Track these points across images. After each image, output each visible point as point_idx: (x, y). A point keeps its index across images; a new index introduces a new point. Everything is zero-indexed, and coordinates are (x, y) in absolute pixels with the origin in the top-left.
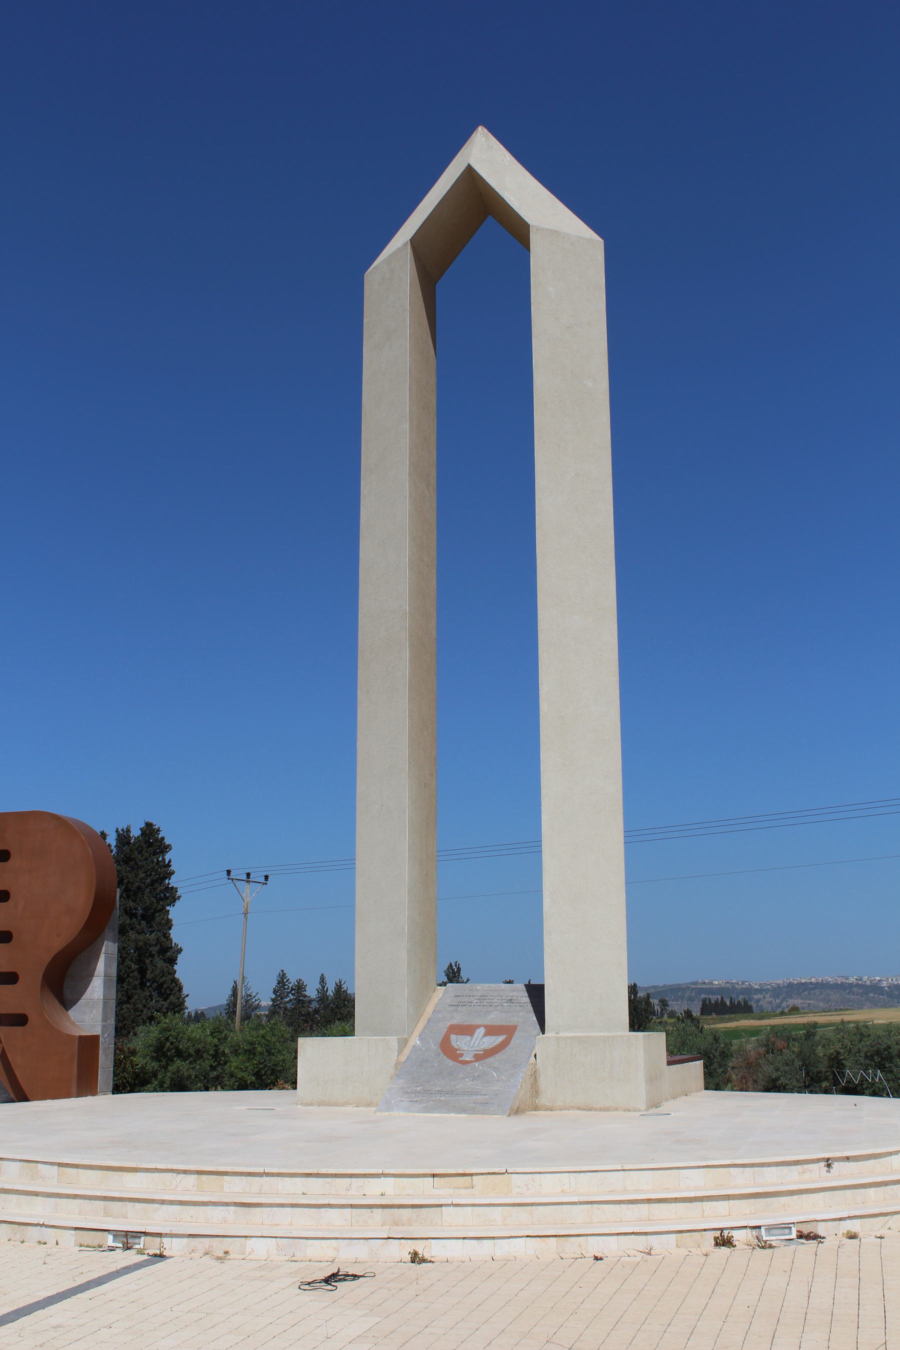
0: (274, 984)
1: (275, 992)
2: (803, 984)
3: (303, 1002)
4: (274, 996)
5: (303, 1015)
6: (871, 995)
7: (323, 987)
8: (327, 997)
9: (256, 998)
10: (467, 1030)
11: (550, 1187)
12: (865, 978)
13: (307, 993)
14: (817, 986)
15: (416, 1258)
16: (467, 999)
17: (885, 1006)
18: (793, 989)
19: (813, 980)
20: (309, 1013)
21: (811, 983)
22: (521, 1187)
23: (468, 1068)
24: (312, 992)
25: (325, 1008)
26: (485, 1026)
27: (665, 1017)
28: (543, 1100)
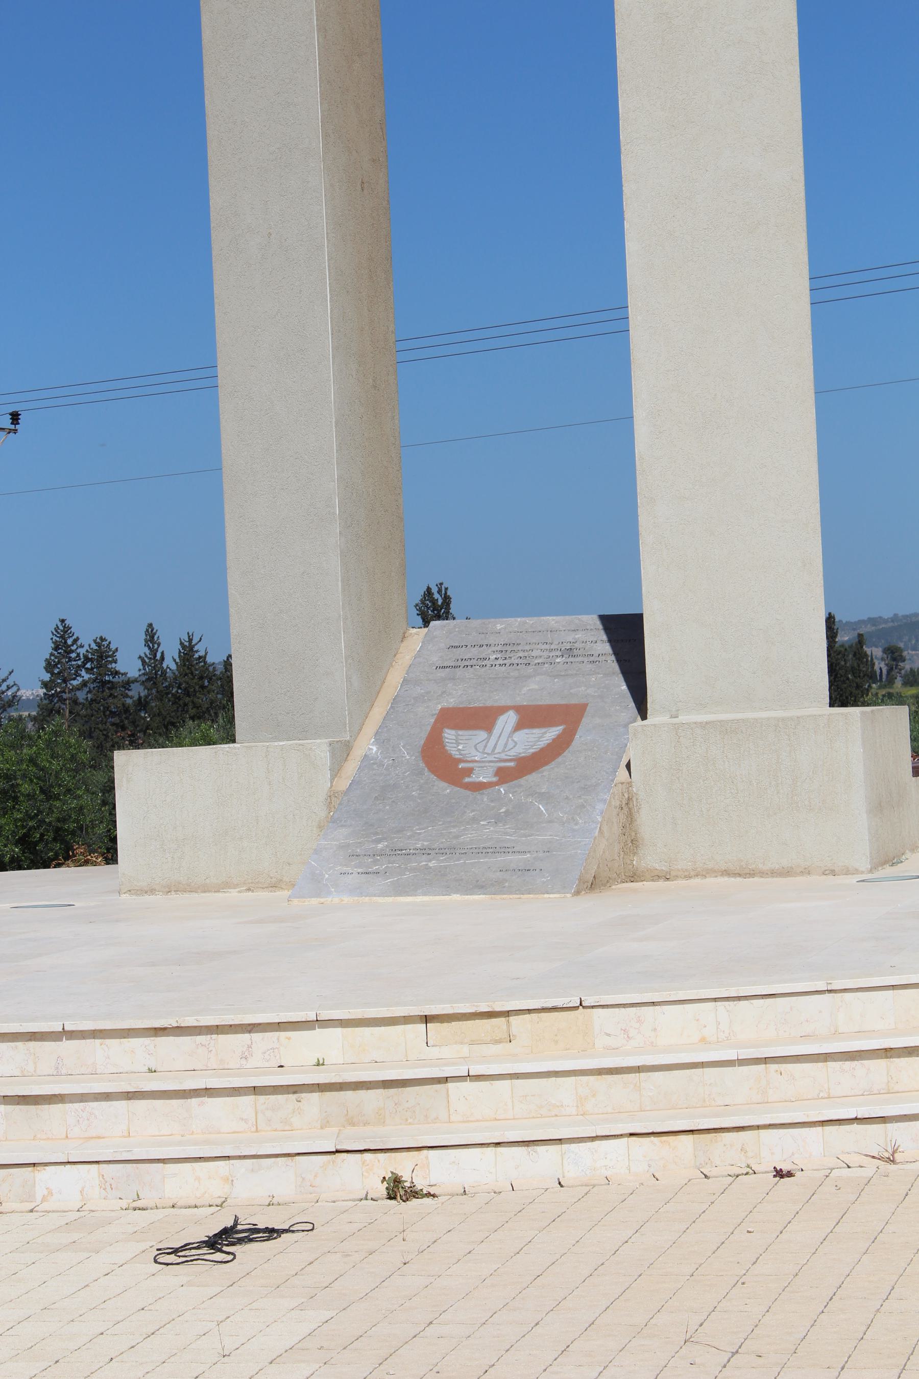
0: (46, 649)
1: (49, 667)
3: (113, 686)
4: (47, 677)
5: (113, 714)
7: (154, 652)
8: (164, 673)
9: (10, 682)
10: (480, 718)
11: (674, 1032)
13: (119, 667)
15: (397, 1190)
16: (474, 652)
20: (126, 710)
22: (612, 1036)
23: (484, 798)
24: (129, 663)
25: (161, 696)
26: (518, 709)
27: (898, 683)
28: (648, 859)
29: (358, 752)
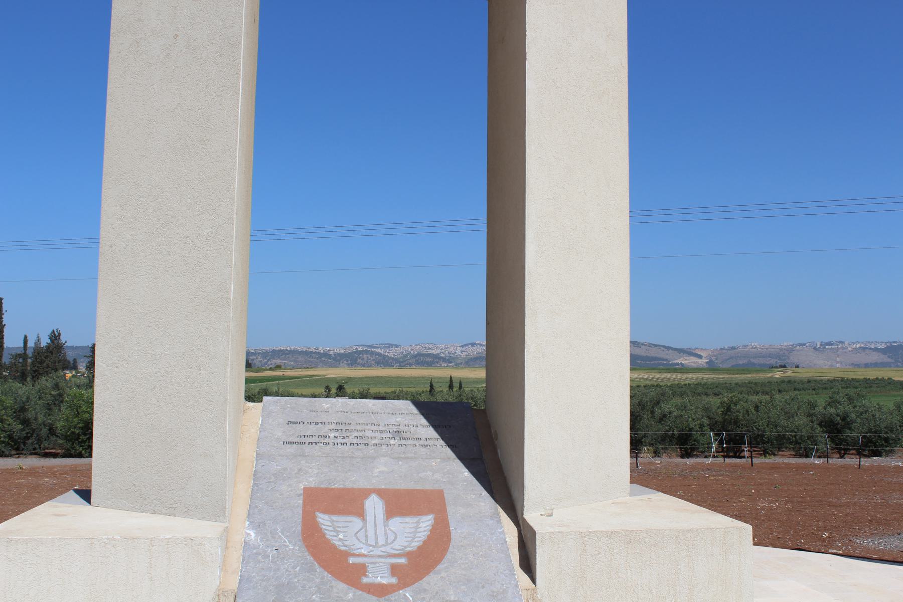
14: (291, 352)
17: (332, 366)
18: (276, 353)
29: (238, 539)
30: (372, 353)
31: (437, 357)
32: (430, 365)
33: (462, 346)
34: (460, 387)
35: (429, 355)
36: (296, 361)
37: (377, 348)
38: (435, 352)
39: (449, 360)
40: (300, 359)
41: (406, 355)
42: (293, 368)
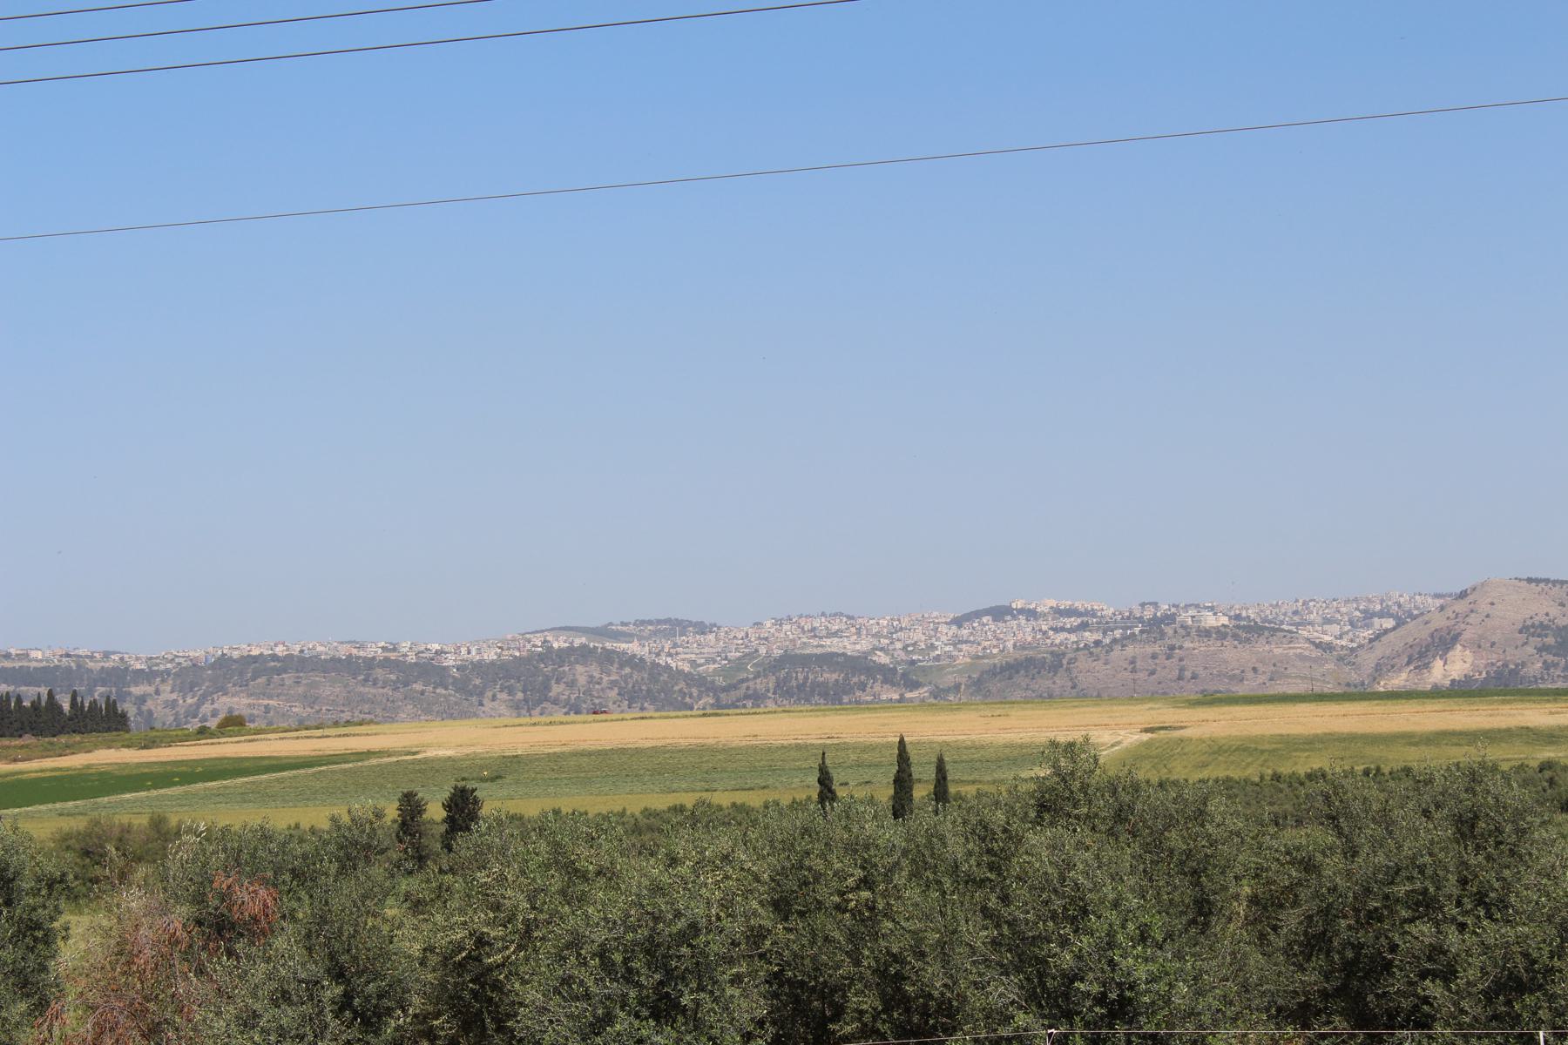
2: (255, 659)
6: (418, 687)
12: (405, 647)
19: (280, 650)
21: (274, 657)
30: (608, 657)
31: (860, 666)
32: (834, 697)
33: (958, 622)
34: (941, 793)
35: (828, 660)
36: (310, 700)
37: (629, 637)
38: (851, 645)
39: (905, 677)
40: (326, 691)
41: (739, 664)
42: (302, 725)
